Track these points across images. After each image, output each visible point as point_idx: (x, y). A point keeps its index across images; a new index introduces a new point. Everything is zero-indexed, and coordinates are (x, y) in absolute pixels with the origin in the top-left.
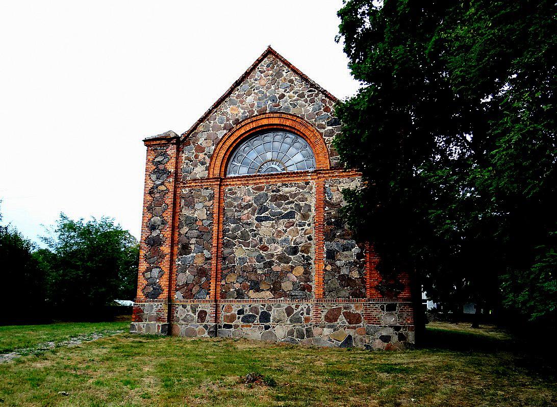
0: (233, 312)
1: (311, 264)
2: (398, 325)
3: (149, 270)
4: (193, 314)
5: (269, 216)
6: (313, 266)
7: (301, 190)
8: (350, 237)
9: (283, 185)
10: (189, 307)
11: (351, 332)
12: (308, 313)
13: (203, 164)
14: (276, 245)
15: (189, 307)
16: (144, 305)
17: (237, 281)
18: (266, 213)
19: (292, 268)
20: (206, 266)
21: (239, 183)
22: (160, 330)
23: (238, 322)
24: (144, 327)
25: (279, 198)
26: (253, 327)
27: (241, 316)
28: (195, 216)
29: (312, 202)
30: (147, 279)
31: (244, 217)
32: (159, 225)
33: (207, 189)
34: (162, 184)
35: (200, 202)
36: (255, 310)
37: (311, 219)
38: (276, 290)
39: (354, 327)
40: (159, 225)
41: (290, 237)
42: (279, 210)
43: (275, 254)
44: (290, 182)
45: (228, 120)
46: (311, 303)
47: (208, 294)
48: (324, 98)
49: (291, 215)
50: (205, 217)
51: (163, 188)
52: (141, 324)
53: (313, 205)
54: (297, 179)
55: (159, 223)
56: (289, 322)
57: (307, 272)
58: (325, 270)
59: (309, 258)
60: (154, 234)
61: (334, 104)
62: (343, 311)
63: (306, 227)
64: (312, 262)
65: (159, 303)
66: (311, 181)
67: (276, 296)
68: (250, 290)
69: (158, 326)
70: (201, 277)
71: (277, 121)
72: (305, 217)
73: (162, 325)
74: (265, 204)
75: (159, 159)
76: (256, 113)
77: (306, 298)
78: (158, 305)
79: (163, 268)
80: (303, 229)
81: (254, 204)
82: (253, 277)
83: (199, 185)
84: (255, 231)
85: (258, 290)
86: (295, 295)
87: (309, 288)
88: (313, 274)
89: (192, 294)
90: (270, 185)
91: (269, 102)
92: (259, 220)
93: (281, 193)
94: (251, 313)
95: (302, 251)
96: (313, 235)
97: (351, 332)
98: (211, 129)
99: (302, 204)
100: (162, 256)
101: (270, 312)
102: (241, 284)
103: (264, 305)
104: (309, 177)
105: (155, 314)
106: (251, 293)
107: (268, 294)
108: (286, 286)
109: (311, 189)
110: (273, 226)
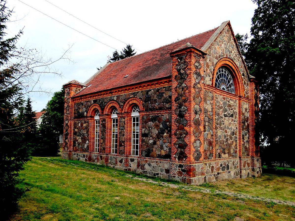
0: (219, 166)
1: (237, 140)
2: (259, 167)
3: (195, 141)
4: (209, 169)
5: (227, 114)
6: (237, 141)
7: (235, 104)
8: (246, 129)
9: (231, 99)
10: (208, 165)
11: (248, 171)
12: (238, 164)
13: (209, 76)
14: (229, 130)
15: (208, 165)
16: (196, 166)
17: (219, 149)
18: (227, 112)
19: (233, 142)
20: (211, 140)
21: (219, 93)
22: (204, 181)
23: (221, 171)
24: (197, 180)
25: (230, 106)
26: (226, 173)
27: (221, 167)
28: (207, 108)
29: (237, 110)
30: (194, 147)
31: (220, 113)
32: (198, 111)
33: (211, 92)
34: (199, 83)
35: (209, 100)
36: (225, 163)
37: (237, 119)
38: (229, 153)
39: (249, 169)
40: (198, 111)
41: (232, 127)
42: (230, 112)
43: (229, 135)
44: (233, 99)
45: (217, 54)
46: (238, 160)
47: (213, 156)
48: (241, 61)
49: (232, 116)
50: (211, 110)
51: (199, 86)
52: (196, 178)
53: (237, 112)
54: (234, 97)
55: (198, 110)
56: (234, 169)
57: (236, 145)
58: (242, 144)
59: (236, 138)
60: (197, 116)
61: (243, 66)
62: (247, 162)
63: (236, 122)
64: (237, 139)
65: (202, 164)
66: (237, 100)
67: (229, 156)
68: (222, 153)
69: (203, 178)
70: (210, 146)
71: (231, 64)
72: (236, 117)
73: (204, 177)
74: (226, 108)
75: (197, 64)
76: (225, 56)
77: (236, 157)
78: (202, 165)
79: (201, 141)
80: (235, 123)
81: (223, 107)
82: (223, 147)
83: (208, 90)
84: (223, 121)
85: (225, 153)
86: (234, 155)
87: (237, 151)
88: (237, 145)
89: (207, 157)
90: (227, 98)
91: (228, 52)
92: (225, 116)
93: (230, 103)
94: (224, 166)
95: (235, 134)
96: (237, 126)
97: (248, 171)
98: (211, 55)
99: (235, 111)
100: (200, 133)
101: (229, 164)
102: (220, 150)
103: (227, 161)
104: (237, 98)
105: (201, 171)
106: (223, 155)
107: (227, 155)
108: (232, 151)
109: (237, 104)
110: (228, 120)
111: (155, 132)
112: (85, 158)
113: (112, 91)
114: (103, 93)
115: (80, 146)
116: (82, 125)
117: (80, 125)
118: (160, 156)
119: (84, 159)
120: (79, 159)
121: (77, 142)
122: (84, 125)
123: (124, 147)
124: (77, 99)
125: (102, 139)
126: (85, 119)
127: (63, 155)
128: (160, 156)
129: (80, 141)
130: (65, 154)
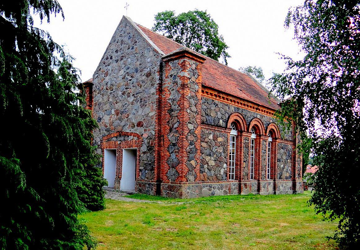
111: (284, 157)
112: (224, 189)
113: (259, 108)
114: (250, 104)
115: (213, 172)
116: (215, 138)
117: (211, 137)
118: (287, 178)
119: (223, 191)
120: (213, 194)
121: (206, 166)
122: (220, 139)
123: (265, 171)
124: (210, 92)
125: (245, 162)
126: (222, 131)
127: (188, 191)
128: (287, 178)
129: (212, 163)
130: (191, 187)
